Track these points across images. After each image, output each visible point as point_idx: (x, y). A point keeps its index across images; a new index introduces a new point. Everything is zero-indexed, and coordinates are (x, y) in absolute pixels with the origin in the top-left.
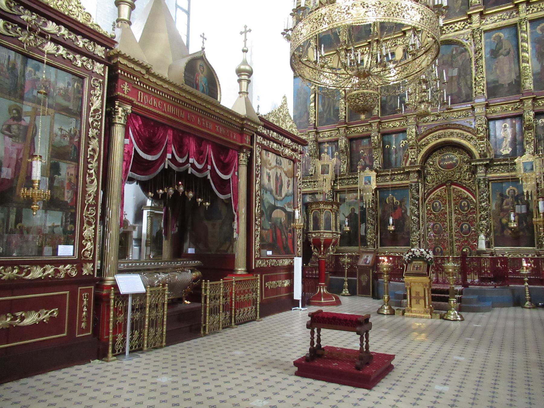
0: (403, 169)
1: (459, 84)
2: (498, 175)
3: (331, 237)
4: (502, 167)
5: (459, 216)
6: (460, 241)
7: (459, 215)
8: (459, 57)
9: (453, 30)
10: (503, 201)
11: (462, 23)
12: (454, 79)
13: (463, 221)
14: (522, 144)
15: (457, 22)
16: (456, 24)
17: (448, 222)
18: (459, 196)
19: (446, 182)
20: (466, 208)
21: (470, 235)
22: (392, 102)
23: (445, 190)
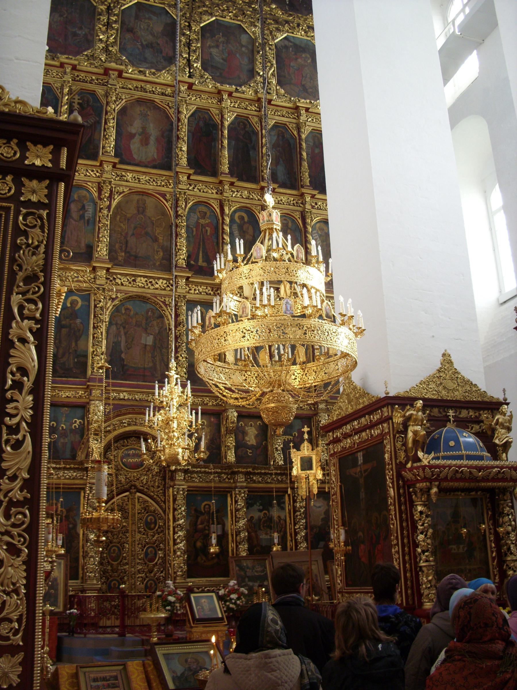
0: (82, 463)
1: (153, 357)
2: (195, 484)
3: (49, 568)
4: (200, 475)
5: (144, 536)
6: (144, 571)
7: (144, 534)
8: (155, 323)
9: (153, 287)
10: (197, 517)
11: (165, 282)
12: (148, 348)
13: (147, 543)
14: (219, 449)
15: (159, 278)
16: (156, 280)
17: (130, 544)
18: (145, 509)
19: (130, 487)
20: (153, 526)
21: (156, 563)
22: (65, 359)
23: (128, 499)
